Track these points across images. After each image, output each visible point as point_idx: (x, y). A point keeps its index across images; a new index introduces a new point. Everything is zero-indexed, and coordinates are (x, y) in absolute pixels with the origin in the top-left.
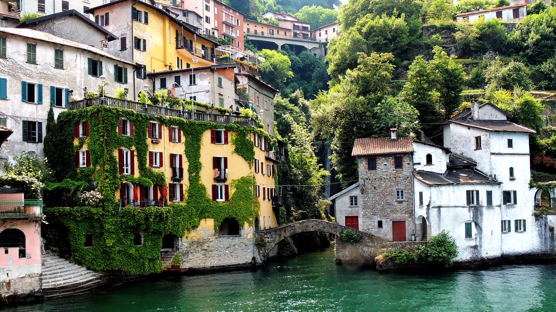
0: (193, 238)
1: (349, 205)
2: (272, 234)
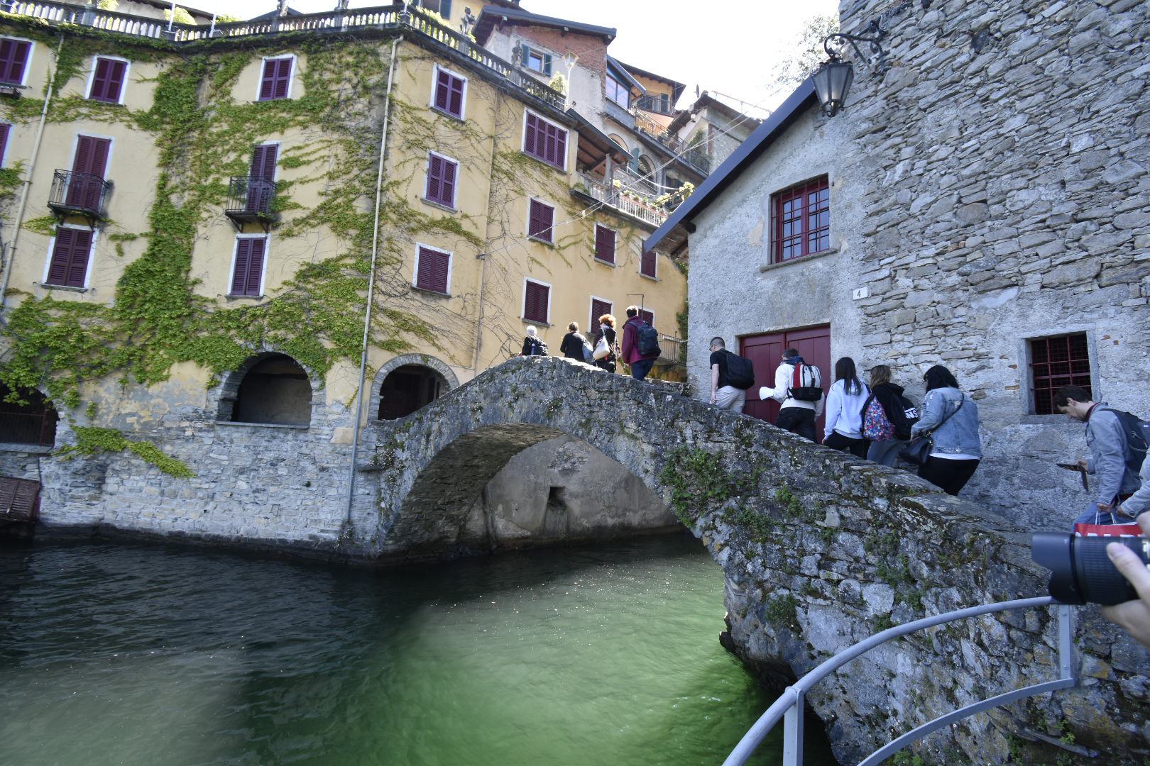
0: (129, 420)
1: (762, 256)
2: (412, 430)
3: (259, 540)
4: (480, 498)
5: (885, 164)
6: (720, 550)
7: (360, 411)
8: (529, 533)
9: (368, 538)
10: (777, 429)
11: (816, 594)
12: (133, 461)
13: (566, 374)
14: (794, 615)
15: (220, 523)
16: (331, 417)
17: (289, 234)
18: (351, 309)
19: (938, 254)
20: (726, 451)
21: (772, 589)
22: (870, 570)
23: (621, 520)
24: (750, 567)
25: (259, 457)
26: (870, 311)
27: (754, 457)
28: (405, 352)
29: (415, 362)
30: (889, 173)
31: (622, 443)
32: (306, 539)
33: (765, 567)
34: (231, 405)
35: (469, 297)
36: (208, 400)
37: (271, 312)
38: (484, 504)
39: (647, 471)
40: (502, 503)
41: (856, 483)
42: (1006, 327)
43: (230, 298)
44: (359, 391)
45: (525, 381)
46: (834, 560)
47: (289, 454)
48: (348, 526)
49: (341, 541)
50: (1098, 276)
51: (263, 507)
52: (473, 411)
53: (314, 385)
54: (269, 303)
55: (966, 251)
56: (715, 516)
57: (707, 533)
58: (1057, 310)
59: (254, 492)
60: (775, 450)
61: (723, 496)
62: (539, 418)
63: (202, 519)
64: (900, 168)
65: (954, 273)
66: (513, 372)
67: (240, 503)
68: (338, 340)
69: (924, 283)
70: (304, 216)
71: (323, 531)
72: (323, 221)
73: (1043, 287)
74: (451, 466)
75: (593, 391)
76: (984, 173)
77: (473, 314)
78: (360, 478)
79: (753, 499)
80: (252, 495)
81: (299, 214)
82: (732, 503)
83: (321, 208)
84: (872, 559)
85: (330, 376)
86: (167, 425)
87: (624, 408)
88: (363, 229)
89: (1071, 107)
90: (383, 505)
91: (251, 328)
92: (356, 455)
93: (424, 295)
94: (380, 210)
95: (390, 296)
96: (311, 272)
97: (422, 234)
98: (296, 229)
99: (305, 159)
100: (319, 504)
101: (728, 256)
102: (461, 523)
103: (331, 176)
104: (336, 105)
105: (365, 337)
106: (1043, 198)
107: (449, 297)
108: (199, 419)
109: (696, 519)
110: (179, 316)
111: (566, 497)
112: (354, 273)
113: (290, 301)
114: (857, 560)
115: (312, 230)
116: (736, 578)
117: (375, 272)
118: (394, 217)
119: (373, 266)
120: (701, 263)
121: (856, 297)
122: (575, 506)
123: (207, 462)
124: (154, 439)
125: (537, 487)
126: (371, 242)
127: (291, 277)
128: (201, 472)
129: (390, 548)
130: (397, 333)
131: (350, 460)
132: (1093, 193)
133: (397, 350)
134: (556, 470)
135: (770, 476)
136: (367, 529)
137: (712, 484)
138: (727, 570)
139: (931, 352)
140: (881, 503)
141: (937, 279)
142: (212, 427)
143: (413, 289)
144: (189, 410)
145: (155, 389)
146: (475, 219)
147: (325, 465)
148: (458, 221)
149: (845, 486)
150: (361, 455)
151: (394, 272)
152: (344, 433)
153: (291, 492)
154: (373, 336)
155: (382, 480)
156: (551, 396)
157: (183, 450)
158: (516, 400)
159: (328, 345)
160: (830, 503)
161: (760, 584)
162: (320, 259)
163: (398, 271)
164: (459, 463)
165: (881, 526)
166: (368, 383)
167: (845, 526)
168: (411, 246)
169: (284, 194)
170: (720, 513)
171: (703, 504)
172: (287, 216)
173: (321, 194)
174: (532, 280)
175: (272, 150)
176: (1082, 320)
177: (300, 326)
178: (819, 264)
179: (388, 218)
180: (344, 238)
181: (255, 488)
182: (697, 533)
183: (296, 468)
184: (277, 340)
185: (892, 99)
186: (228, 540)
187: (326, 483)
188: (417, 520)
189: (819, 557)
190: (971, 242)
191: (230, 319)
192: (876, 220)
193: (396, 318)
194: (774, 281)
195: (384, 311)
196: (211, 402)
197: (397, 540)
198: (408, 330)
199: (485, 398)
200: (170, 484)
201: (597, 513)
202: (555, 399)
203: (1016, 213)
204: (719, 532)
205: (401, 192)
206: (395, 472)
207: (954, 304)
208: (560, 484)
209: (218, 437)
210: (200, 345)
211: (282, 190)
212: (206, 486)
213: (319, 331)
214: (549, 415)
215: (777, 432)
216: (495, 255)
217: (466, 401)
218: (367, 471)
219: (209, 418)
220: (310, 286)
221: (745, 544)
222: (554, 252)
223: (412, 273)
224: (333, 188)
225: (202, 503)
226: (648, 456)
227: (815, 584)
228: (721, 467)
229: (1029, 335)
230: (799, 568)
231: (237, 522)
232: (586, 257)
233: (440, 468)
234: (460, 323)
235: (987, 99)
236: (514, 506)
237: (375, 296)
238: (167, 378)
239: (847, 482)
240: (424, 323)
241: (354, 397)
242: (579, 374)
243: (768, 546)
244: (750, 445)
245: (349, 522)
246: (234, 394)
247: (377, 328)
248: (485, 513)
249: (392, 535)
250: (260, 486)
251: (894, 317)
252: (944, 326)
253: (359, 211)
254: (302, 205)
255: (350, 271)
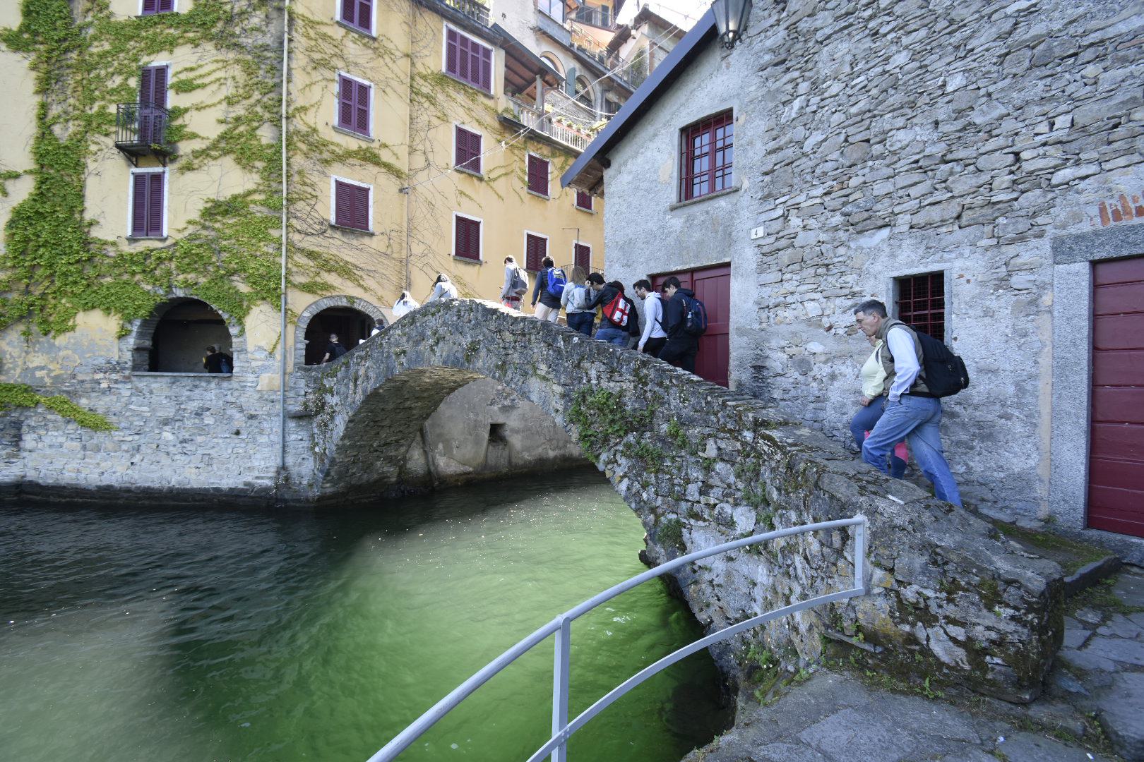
2: (339, 374)
3: (192, 489)
4: (418, 438)
5: (784, 100)
6: (620, 481)
7: (285, 357)
8: (471, 469)
9: (305, 482)
10: (671, 367)
11: (697, 516)
12: (49, 417)
13: (483, 316)
14: (680, 535)
15: (148, 475)
16: (254, 364)
17: (189, 168)
18: (265, 249)
19: (825, 194)
20: (625, 390)
21: (663, 514)
22: (739, 495)
23: (562, 452)
24: (645, 496)
25: (182, 407)
26: (766, 250)
27: (649, 395)
28: (328, 294)
29: (340, 304)
30: (787, 109)
31: (535, 384)
32: (241, 486)
33: (658, 495)
34: (146, 355)
35: (393, 234)
36: (120, 350)
37: (178, 254)
38: (424, 443)
39: (557, 411)
40: (443, 442)
41: (730, 417)
42: (878, 267)
43: (132, 240)
44: (282, 337)
45: (444, 324)
46: (712, 487)
47: (214, 402)
48: (283, 472)
49: (277, 487)
50: (959, 217)
51: (192, 457)
52: (398, 355)
53: (233, 331)
54: (175, 244)
55: (848, 191)
56: (616, 451)
57: (609, 467)
58: (921, 251)
59: (181, 442)
60: (667, 388)
61: (622, 433)
62: (458, 361)
63: (129, 472)
64: (797, 104)
65: (838, 213)
66: (433, 315)
67: (168, 454)
68: (254, 283)
69: (812, 223)
70: (204, 147)
71: (257, 478)
72: (226, 152)
73: (911, 227)
74: (383, 410)
75: (508, 333)
76: (869, 111)
77: (400, 252)
78: (292, 424)
79: (648, 434)
80: (179, 445)
81: (197, 145)
82: (631, 438)
83: (222, 137)
84: (741, 485)
85: (249, 321)
86: (80, 377)
87: (536, 350)
88: (270, 161)
89: (950, 44)
90: (317, 449)
91: (158, 272)
92: (284, 401)
93: (344, 232)
94: (287, 140)
95: (307, 234)
96: (216, 210)
97: (337, 166)
98: (196, 161)
99: (199, 82)
100: (251, 452)
101: (641, 193)
102: (401, 463)
103: (230, 101)
104: (230, 20)
105: (283, 280)
106: (918, 138)
107: (372, 235)
108: (114, 370)
109: (600, 454)
110: (78, 262)
111: (507, 433)
112: (264, 209)
113: (197, 242)
114: (729, 486)
115: (214, 162)
116: (633, 505)
117: (288, 209)
118: (304, 147)
119: (285, 202)
120: (615, 200)
121: (754, 237)
122: (516, 441)
123: (128, 414)
124: (68, 392)
125: (477, 425)
126: (281, 175)
127: (195, 216)
128: (123, 425)
129: (328, 491)
130: (318, 274)
131: (279, 407)
132: (961, 134)
133: (320, 292)
134: (496, 408)
135: (662, 413)
136: (303, 473)
137: (613, 421)
138: (626, 499)
139: (815, 290)
140: (748, 435)
141: (823, 219)
142: (128, 378)
143: (332, 227)
144: (101, 361)
145: (61, 340)
146: (395, 149)
147: (253, 413)
148: (376, 151)
149: (722, 420)
150: (290, 401)
151: (308, 208)
152: (270, 379)
153: (221, 441)
154: (291, 278)
155: (315, 425)
156: (469, 340)
157: (101, 403)
158: (437, 343)
159: (244, 288)
160: (710, 436)
161: (653, 510)
162: (225, 195)
163: (313, 206)
164: (391, 406)
165: (748, 456)
166: (291, 328)
167: (721, 457)
168: (326, 180)
169: (179, 122)
170: (620, 448)
171: (606, 439)
172: (185, 148)
173: (221, 122)
174: (461, 215)
175: (162, 71)
176: (942, 260)
177: (211, 269)
178: (722, 203)
179: (297, 148)
180: (251, 171)
181: (181, 438)
182: (601, 467)
183: (222, 417)
184: (187, 285)
185: (790, 28)
186: (160, 491)
187: (256, 430)
188: (354, 462)
189: (700, 484)
190: (854, 182)
191: (134, 263)
192: (774, 158)
193: (315, 259)
194: (682, 220)
195: (301, 250)
196: (124, 351)
197: (332, 481)
198: (329, 271)
199: (408, 342)
200: (91, 438)
201: (538, 447)
202: (473, 342)
203: (894, 153)
204: (619, 465)
205: (310, 118)
206: (326, 417)
207: (836, 244)
208: (500, 421)
209: (137, 389)
210: (104, 292)
211: (177, 118)
212: (130, 438)
213: (233, 274)
214: (468, 359)
215: (671, 370)
216: (419, 188)
217: (389, 344)
218: (298, 417)
219: (123, 369)
220: (217, 225)
221: (641, 475)
222: (484, 184)
223: (329, 209)
224: (233, 115)
225: (128, 455)
226: (558, 396)
227: (697, 508)
228: (620, 405)
229: (896, 274)
230: (684, 495)
231: (167, 473)
232: (518, 189)
233: (372, 411)
234: (386, 262)
235: (876, 33)
236: (455, 444)
237: (291, 235)
238: (73, 328)
239: (724, 417)
240: (347, 263)
241: (277, 343)
242: (494, 317)
243: (660, 476)
244: (645, 384)
245: (284, 467)
246: (148, 343)
247: (294, 269)
248: (425, 453)
249: (329, 478)
250: (187, 437)
251: (785, 256)
252: (827, 265)
253: (265, 141)
254: (201, 134)
255: (259, 208)
